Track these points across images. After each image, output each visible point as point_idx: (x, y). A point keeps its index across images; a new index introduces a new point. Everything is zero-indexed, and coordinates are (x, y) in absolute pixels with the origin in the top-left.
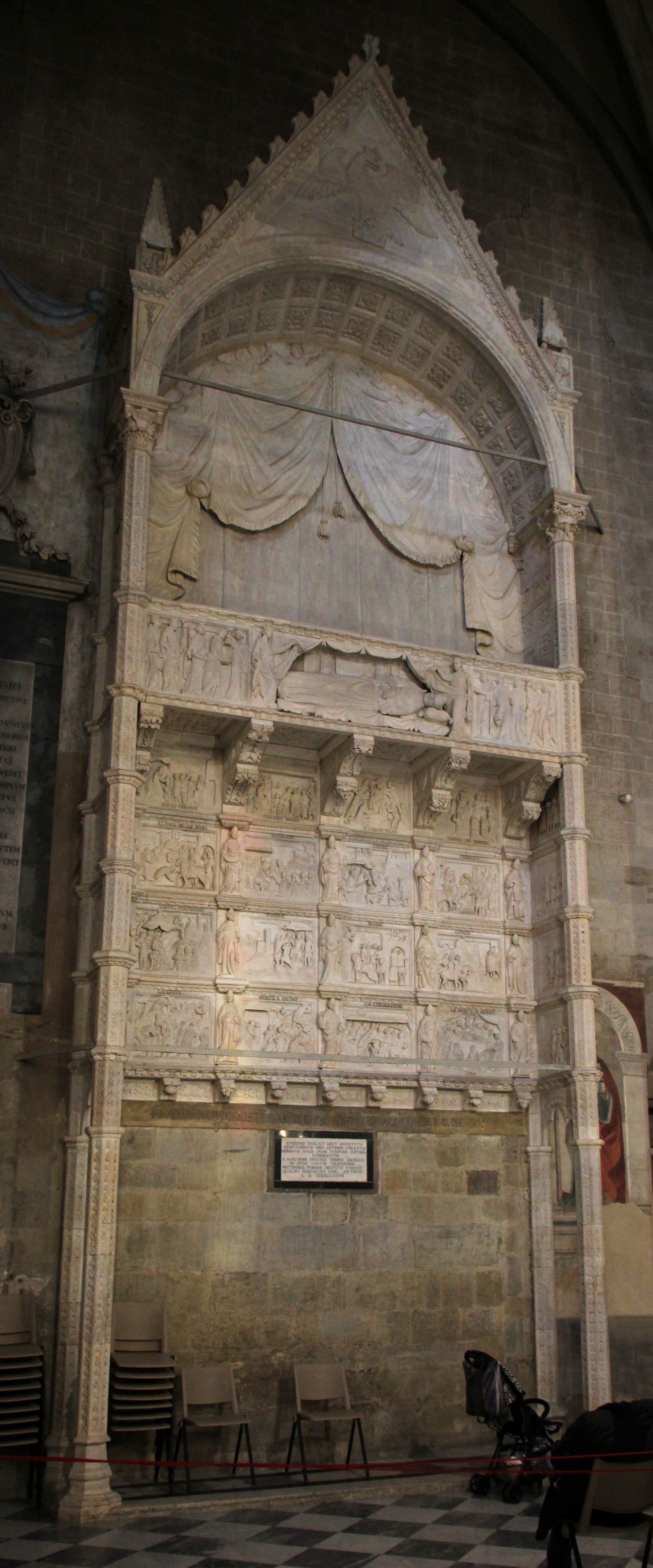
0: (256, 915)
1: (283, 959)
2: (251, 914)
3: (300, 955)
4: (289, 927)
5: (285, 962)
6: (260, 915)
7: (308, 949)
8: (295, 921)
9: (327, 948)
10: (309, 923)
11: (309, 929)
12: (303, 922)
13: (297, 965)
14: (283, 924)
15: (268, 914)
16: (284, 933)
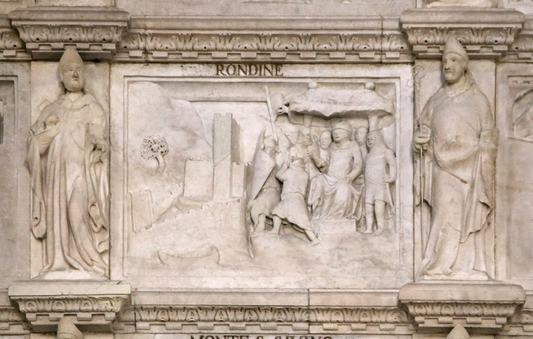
0: (175, 71)
1: (280, 212)
2: (156, 71)
3: (343, 193)
4: (301, 105)
5: (286, 223)
6: (189, 71)
7: (375, 171)
8: (322, 82)
9: (436, 161)
10: (378, 86)
11: (379, 105)
12: (355, 83)
13: (331, 229)
14: (278, 98)
15: (219, 64)
16: (289, 128)
